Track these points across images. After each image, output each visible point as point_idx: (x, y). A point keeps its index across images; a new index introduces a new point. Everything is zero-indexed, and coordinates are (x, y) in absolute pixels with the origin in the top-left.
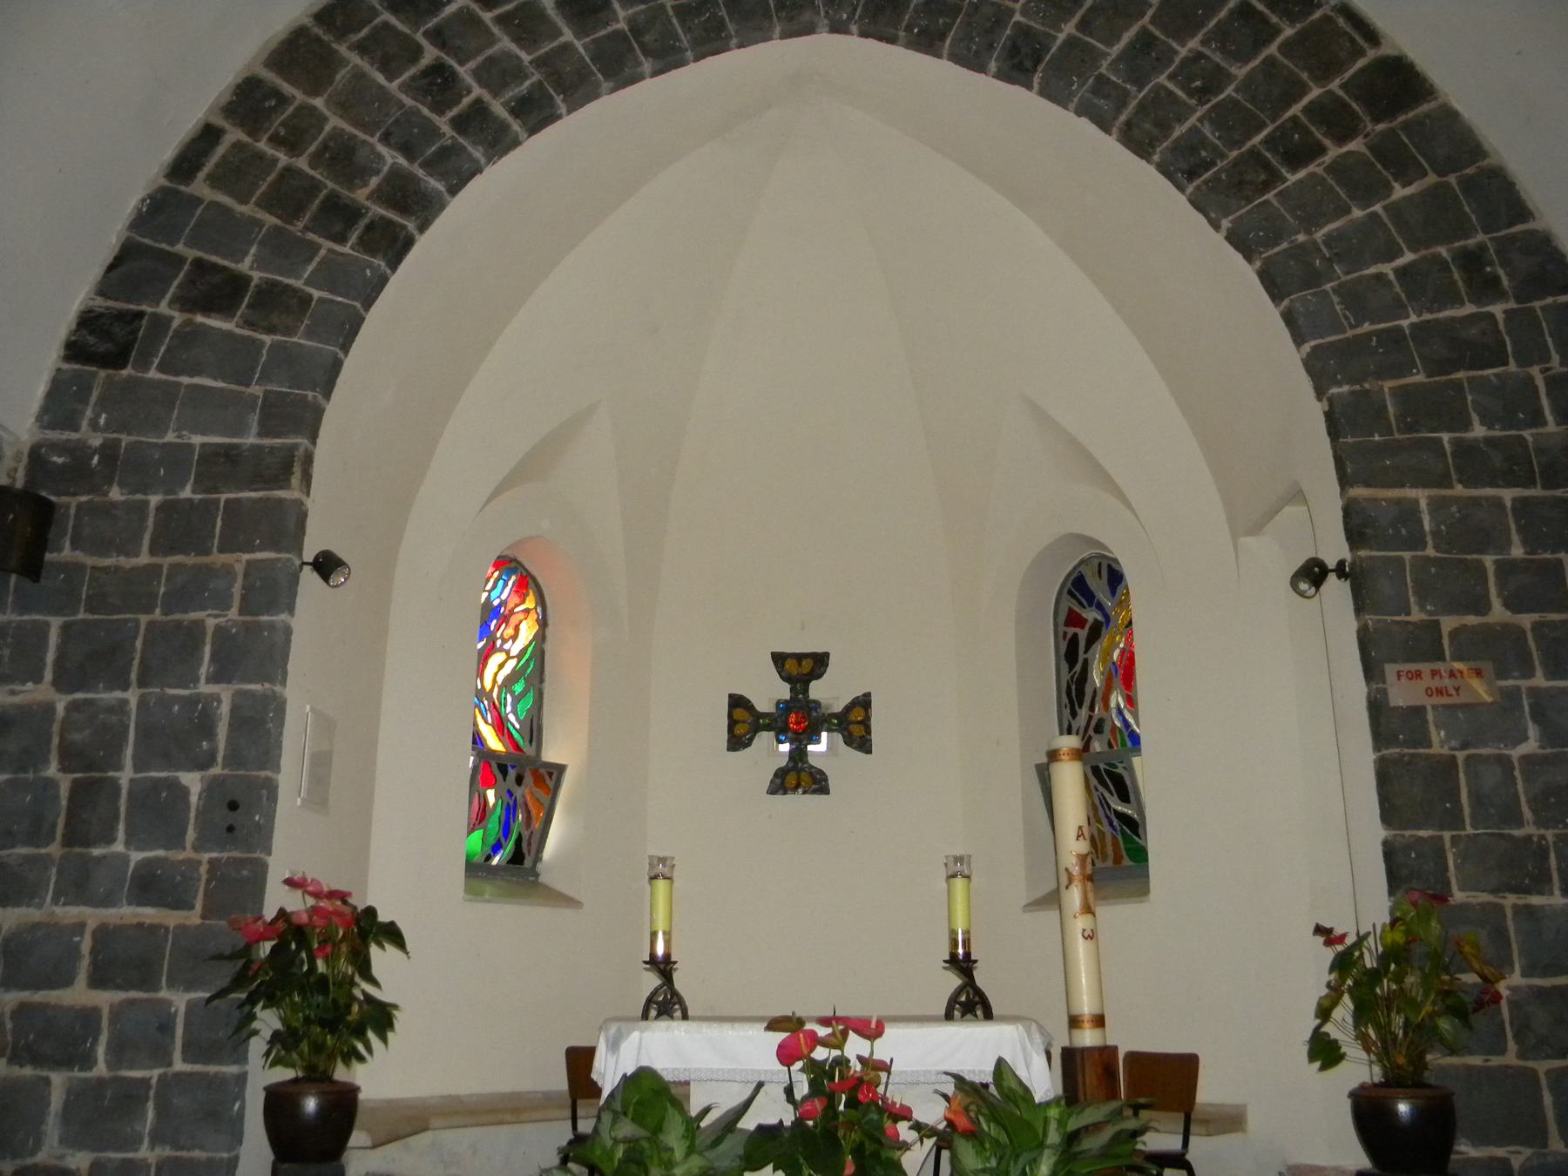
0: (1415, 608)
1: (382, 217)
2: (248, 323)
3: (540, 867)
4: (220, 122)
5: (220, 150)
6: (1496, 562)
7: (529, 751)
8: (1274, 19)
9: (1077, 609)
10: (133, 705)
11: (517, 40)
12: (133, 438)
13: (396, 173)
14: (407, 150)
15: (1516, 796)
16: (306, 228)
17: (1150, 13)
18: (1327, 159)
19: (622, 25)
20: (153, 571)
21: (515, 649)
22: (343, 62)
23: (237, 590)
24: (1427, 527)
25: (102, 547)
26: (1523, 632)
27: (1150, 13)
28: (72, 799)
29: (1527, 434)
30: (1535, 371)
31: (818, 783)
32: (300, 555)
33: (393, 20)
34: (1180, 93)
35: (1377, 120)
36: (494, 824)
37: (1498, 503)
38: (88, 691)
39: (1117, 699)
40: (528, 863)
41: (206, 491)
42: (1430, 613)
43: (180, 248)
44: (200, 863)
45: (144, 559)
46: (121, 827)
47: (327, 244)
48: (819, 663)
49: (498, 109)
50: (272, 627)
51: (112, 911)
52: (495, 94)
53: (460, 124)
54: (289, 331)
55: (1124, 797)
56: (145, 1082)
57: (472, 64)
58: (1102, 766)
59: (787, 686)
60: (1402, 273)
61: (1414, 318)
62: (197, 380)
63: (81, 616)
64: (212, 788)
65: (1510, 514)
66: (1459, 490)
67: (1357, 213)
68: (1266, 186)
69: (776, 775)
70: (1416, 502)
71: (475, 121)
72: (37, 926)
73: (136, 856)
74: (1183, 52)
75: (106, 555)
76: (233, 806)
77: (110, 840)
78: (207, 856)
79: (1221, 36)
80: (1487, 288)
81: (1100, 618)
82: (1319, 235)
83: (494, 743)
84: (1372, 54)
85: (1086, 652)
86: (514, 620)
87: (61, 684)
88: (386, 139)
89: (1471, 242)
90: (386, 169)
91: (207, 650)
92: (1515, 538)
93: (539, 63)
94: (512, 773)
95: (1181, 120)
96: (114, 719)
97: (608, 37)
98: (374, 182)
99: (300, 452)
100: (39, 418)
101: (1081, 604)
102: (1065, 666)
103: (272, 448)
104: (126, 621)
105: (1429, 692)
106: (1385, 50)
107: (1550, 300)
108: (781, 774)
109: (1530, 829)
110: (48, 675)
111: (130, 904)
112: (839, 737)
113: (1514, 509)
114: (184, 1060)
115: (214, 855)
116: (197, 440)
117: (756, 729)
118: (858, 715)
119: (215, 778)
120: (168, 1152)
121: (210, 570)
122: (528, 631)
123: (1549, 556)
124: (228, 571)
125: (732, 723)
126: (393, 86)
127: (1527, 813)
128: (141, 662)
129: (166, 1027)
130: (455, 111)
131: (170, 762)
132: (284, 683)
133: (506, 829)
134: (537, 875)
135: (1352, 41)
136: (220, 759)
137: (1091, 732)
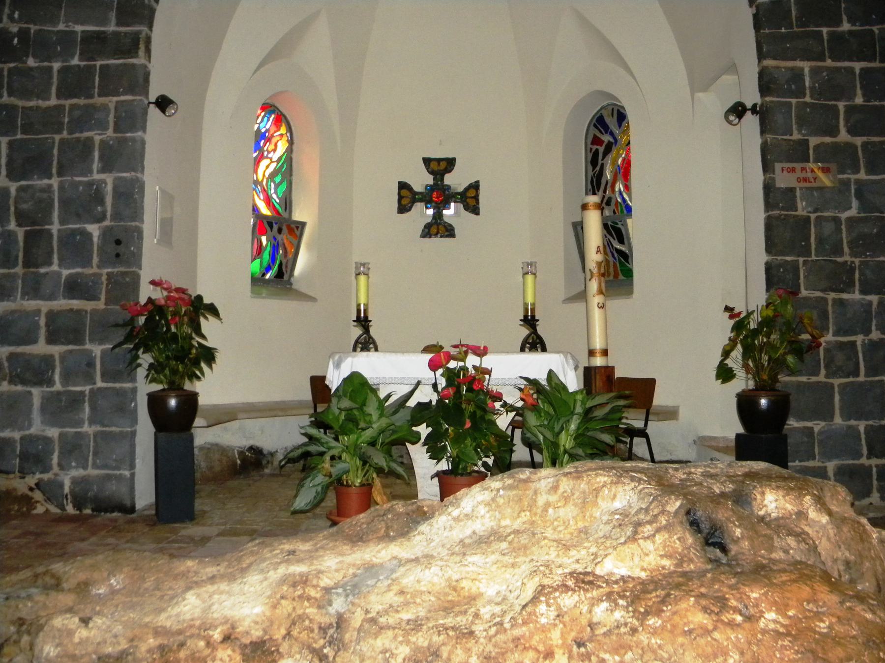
0: (795, 132)
3: (292, 280)
6: (845, 106)
7: (285, 215)
9: (599, 135)
10: (56, 187)
12: (37, 27)
15: (841, 240)
20: (59, 108)
21: (275, 156)
23: (111, 119)
24: (807, 84)
26: (856, 147)
31: (449, 232)
32: (147, 97)
36: (266, 256)
37: (851, 70)
38: (28, 180)
39: (619, 186)
40: (286, 277)
41: (88, 60)
42: (804, 135)
44: (101, 275)
45: (53, 101)
46: (55, 256)
48: (450, 163)
50: (134, 140)
51: (55, 303)
55: (621, 241)
56: (82, 393)
58: (610, 223)
59: (432, 177)
63: (19, 136)
64: (106, 233)
65: (858, 78)
66: (829, 63)
69: (425, 227)
70: (802, 69)
72: (13, 312)
73: (65, 272)
75: (30, 100)
76: (118, 242)
77: (50, 264)
78: (105, 271)
81: (611, 140)
83: (265, 211)
85: (602, 160)
86: (274, 140)
91: (96, 154)
92: (859, 92)
94: (275, 227)
96: (45, 195)
99: (143, 36)
101: (601, 132)
102: (590, 168)
103: (126, 33)
104: (47, 138)
105: (799, 180)
108: (428, 226)
109: (847, 258)
111: (65, 299)
112: (461, 206)
113: (860, 74)
114: (103, 381)
115: (110, 270)
116: (79, 28)
117: (414, 201)
118: (472, 193)
119: (107, 226)
121: (93, 107)
122: (282, 146)
123: (877, 103)
124: (105, 108)
125: (400, 198)
127: (846, 249)
128: (58, 163)
129: (91, 364)
131: (79, 217)
132: (142, 171)
133: (273, 259)
134: (291, 284)
136: (109, 216)
137: (604, 205)
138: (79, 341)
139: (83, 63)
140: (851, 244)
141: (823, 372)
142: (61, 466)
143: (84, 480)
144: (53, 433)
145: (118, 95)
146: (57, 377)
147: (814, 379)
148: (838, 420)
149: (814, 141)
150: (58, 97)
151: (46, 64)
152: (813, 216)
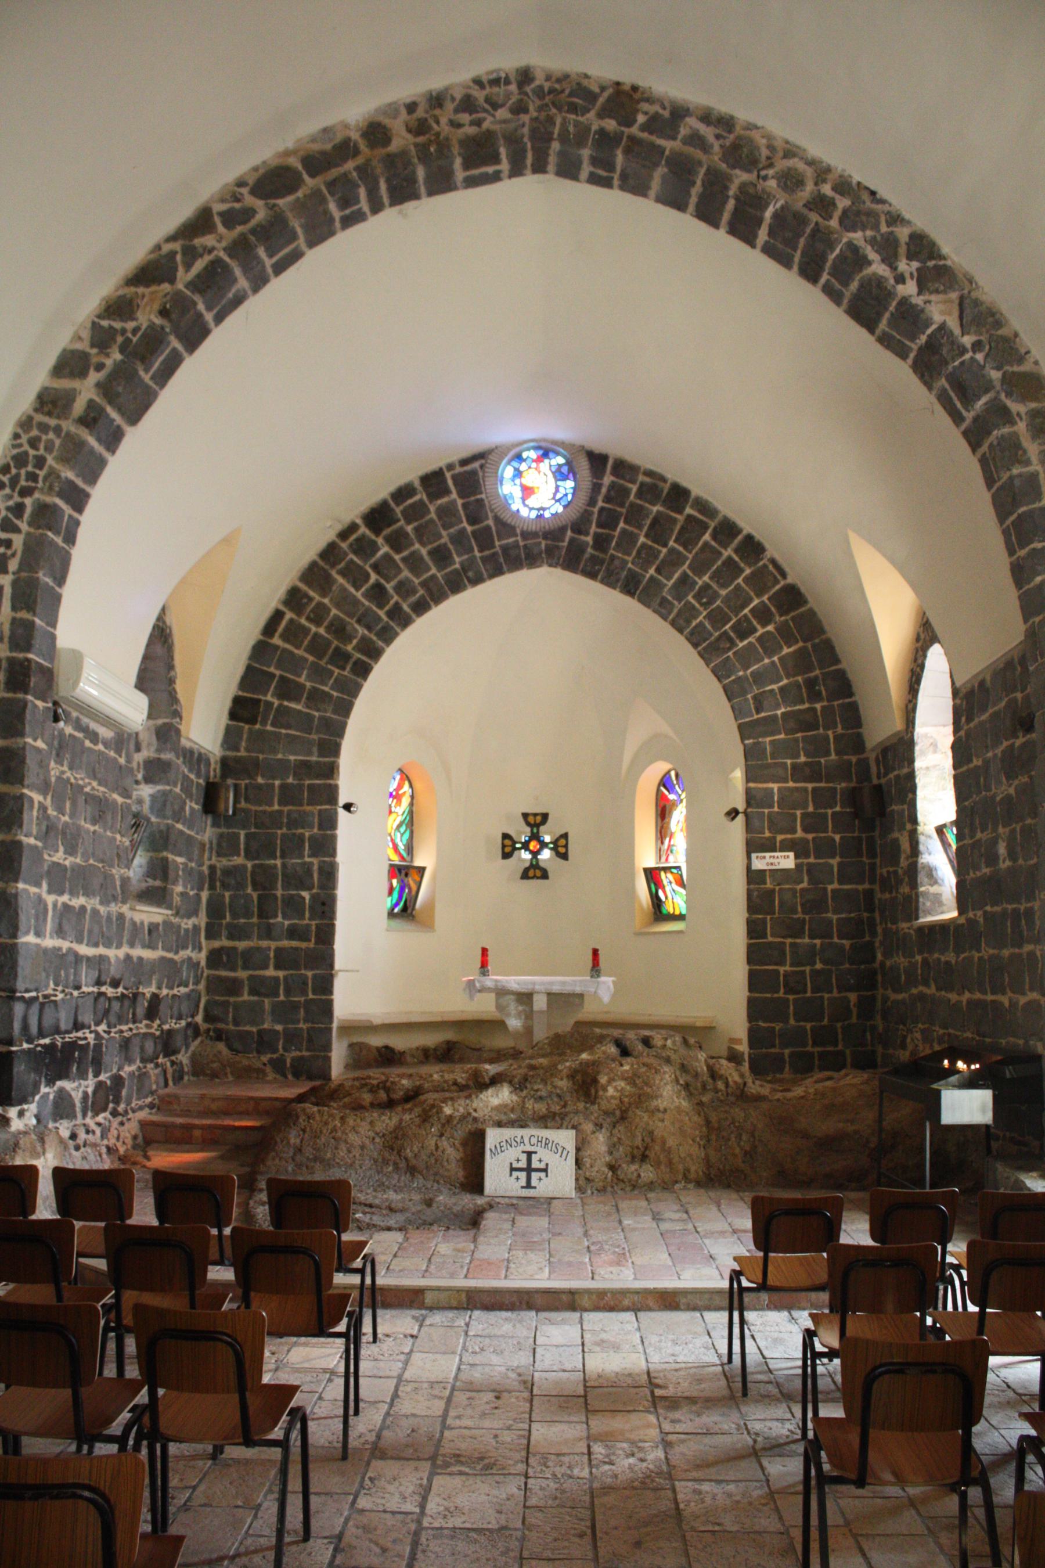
0: (766, 831)
1: (359, 659)
2: (308, 707)
4: (282, 608)
8: (742, 565)
13: (364, 638)
14: (369, 628)
16: (327, 663)
17: (688, 563)
18: (758, 634)
19: (457, 566)
20: (280, 812)
22: (335, 581)
23: (316, 820)
24: (776, 799)
27: (688, 563)
28: (259, 902)
29: (822, 760)
30: (830, 733)
31: (545, 875)
33: (355, 559)
34: (697, 605)
35: (781, 616)
36: (396, 895)
37: (806, 789)
40: (409, 911)
43: (272, 670)
45: (276, 807)
47: (337, 671)
48: (545, 817)
49: (406, 607)
52: (404, 600)
53: (390, 614)
54: (325, 711)
57: (393, 583)
60: (782, 689)
61: (783, 710)
62: (289, 732)
63: (253, 830)
64: (313, 897)
66: (791, 784)
67: (766, 661)
68: (730, 649)
70: (772, 789)
72: (251, 948)
73: (287, 923)
74: (700, 583)
76: (323, 904)
77: (276, 916)
78: (314, 923)
80: (814, 696)
82: (749, 672)
84: (782, 583)
87: (248, 856)
88: (359, 621)
89: (812, 675)
90: (360, 635)
91: (307, 845)
93: (424, 584)
94: (403, 872)
95: (695, 618)
97: (451, 572)
98: (355, 642)
100: (222, 745)
102: (659, 819)
103: (325, 763)
106: (790, 580)
107: (841, 701)
109: (800, 915)
110: (242, 853)
112: (553, 853)
116: (292, 758)
117: (515, 849)
118: (562, 842)
120: (310, 1025)
121: (305, 812)
122: (406, 801)
125: (504, 846)
126: (359, 595)
129: (305, 983)
130: (387, 608)
135: (775, 577)
138: (297, 968)
139: (295, 782)
140: (802, 905)
141: (782, 990)
142: (285, 1049)
143: (302, 1058)
144: (279, 1027)
145: (321, 804)
146: (281, 992)
147: (776, 995)
148: (792, 1022)
149: (779, 838)
150: (280, 804)
151: (271, 781)
152: (777, 888)
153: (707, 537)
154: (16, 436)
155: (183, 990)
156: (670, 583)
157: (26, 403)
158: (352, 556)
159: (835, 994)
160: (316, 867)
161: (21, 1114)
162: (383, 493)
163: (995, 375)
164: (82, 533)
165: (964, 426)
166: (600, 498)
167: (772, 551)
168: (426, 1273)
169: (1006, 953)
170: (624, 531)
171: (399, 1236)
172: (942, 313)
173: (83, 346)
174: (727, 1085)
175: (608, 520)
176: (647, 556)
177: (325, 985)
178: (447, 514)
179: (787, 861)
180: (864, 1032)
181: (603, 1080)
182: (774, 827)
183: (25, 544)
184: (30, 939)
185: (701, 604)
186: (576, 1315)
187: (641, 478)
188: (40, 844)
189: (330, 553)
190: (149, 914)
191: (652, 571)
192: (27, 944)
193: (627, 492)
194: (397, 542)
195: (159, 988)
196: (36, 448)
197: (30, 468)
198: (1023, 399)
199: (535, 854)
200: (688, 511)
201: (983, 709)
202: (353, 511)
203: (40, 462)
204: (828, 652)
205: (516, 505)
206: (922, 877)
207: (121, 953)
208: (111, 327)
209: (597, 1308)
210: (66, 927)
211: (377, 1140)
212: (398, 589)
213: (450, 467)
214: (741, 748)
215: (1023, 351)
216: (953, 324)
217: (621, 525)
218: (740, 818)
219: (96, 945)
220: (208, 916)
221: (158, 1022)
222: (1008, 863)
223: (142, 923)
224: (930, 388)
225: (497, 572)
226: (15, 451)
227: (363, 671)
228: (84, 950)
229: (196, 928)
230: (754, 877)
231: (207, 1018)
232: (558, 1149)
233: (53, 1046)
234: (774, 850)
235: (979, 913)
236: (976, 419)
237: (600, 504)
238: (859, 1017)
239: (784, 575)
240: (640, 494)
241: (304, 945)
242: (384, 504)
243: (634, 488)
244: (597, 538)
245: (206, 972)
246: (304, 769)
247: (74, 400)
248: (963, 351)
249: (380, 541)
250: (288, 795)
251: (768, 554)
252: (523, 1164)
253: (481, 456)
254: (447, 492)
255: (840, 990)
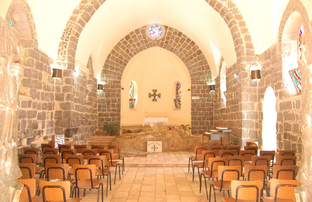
2: (116, 71)
5: (111, 56)
11: (133, 47)
18: (194, 59)
25: (107, 88)
35: (198, 55)
37: (201, 86)
43: (109, 64)
45: (110, 89)
48: (156, 90)
49: (132, 53)
52: (132, 52)
53: (130, 55)
55: (180, 102)
57: (130, 49)
64: (117, 104)
66: (199, 85)
71: (131, 55)
73: (112, 108)
79: (187, 48)
84: (198, 50)
87: (106, 97)
88: (124, 56)
106: (199, 49)
108: (153, 100)
122: (132, 87)
126: (124, 51)
129: (115, 119)
148: (199, 125)
153: (185, 41)
154: (67, 24)
155: (94, 120)
156: (179, 50)
157: (68, 19)
158: (123, 44)
159: (206, 121)
160: (117, 99)
161: (71, 139)
162: (128, 33)
163: (234, 15)
164: (79, 42)
165: (228, 24)
166: (167, 34)
167: (197, 44)
168: (138, 162)
169: (234, 113)
170: (171, 40)
171: (134, 158)
172: (225, 4)
173: (78, 8)
174: (187, 135)
175: (168, 39)
176: (175, 45)
177: (119, 119)
178: (139, 37)
179: (198, 98)
180: (211, 127)
181: (167, 134)
182: (196, 92)
183: (69, 43)
184: (72, 110)
185: (184, 53)
186: (162, 168)
187: (174, 31)
188: (73, 94)
189: (119, 44)
190: (89, 107)
191: (175, 47)
192: (72, 111)
193: (171, 33)
194: (131, 42)
195: (91, 119)
196: (71, 27)
197: (70, 30)
198: (238, 19)
199: (155, 97)
200: (182, 36)
201: (231, 72)
202: (123, 36)
203: (71, 29)
204: (206, 62)
205: (152, 35)
206: (221, 101)
207: (85, 113)
208: (83, 5)
209: (166, 167)
210: (77, 109)
211: (130, 143)
212: (131, 50)
213: (140, 28)
214: (191, 78)
215: (238, 11)
216: (227, 7)
217: (170, 39)
218: (190, 90)
219: (81, 112)
220: (98, 107)
221: (90, 125)
222: (234, 98)
223: (88, 108)
224: (223, 17)
225: (148, 47)
226: (67, 27)
227: (125, 65)
228: (79, 113)
229: (96, 109)
230: (193, 101)
231: (99, 125)
232: (159, 144)
233: (75, 128)
234: (196, 96)
235: (230, 106)
236: (230, 23)
237: (167, 35)
238: (210, 125)
239: (198, 48)
240: (173, 34)
241: (115, 112)
242: (129, 35)
243: (173, 32)
244: (166, 41)
245: (98, 117)
246: (115, 82)
247: (77, 18)
248: (228, 11)
249: (128, 41)
250: (113, 87)
251: (196, 44)
252: (154, 147)
253: (146, 26)
254: (140, 33)
255: (207, 120)
